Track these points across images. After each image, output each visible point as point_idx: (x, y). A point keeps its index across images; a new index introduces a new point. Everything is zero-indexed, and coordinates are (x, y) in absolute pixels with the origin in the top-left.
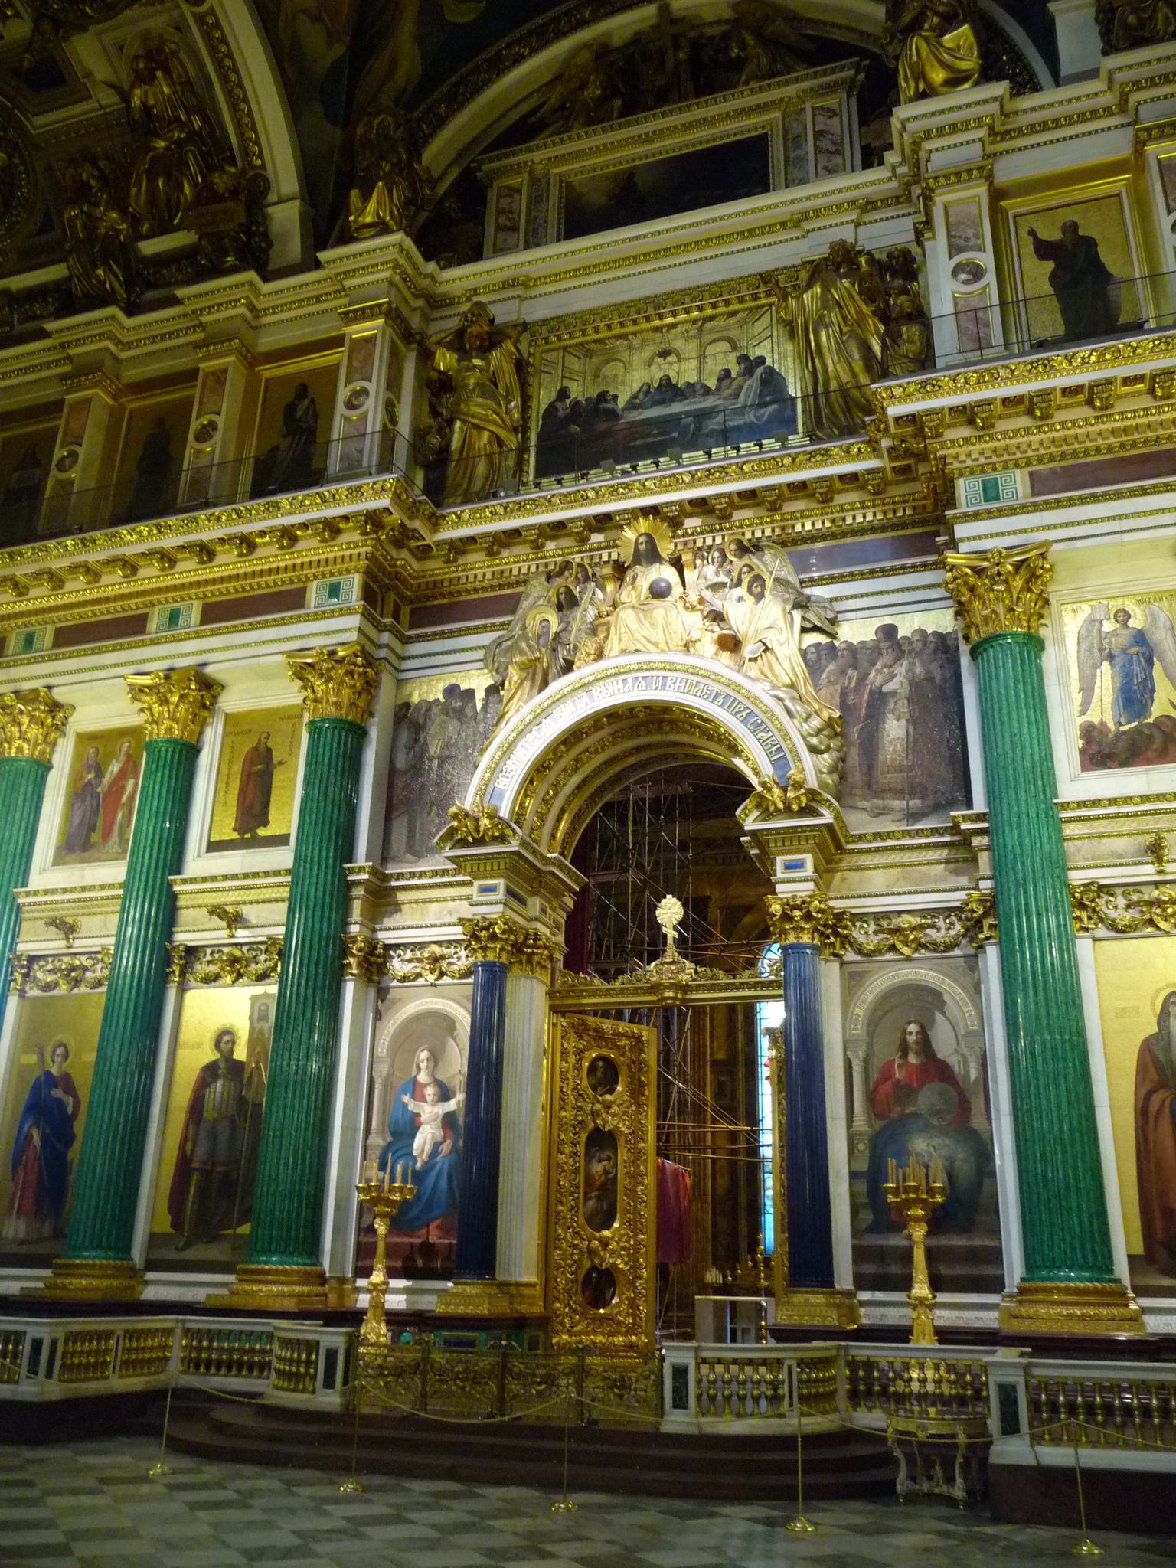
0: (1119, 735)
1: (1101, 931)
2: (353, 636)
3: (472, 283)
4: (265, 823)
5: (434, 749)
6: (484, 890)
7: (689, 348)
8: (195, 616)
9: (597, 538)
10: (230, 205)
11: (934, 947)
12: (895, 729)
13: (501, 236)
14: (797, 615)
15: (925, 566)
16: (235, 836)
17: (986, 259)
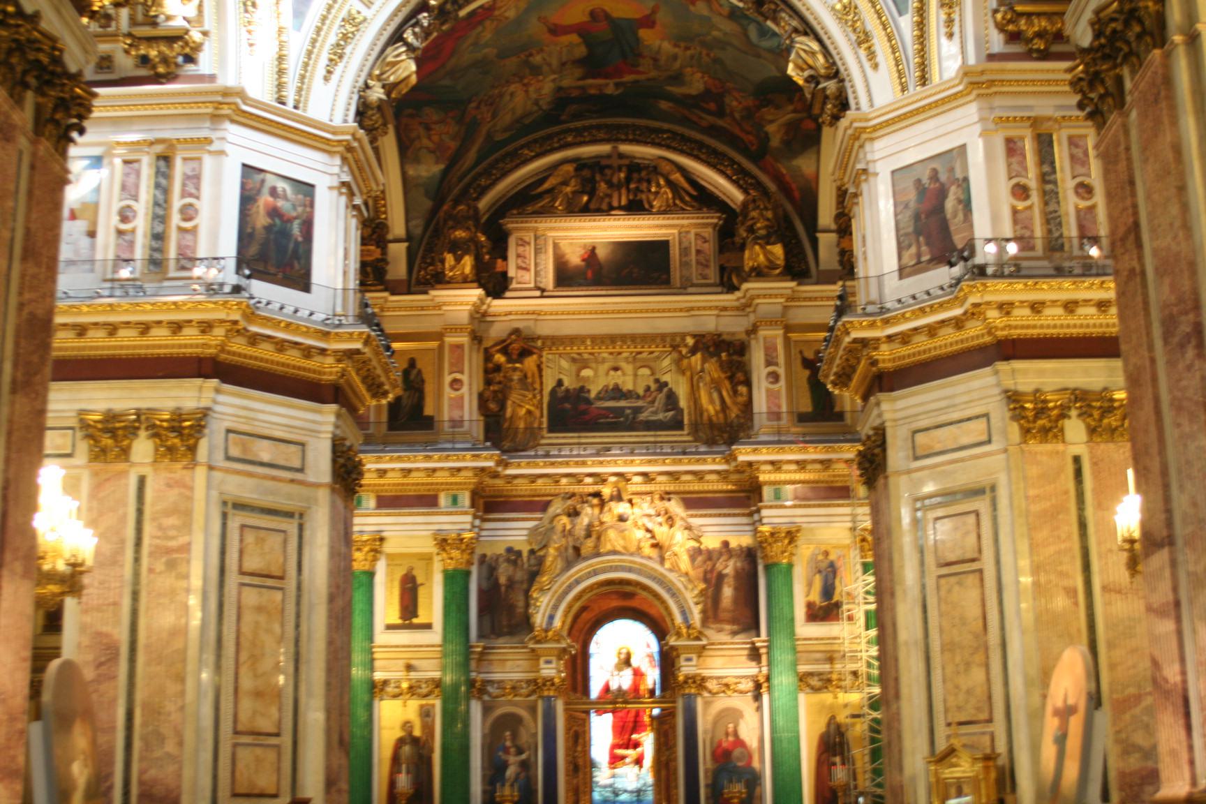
0: (821, 608)
1: (808, 690)
2: (468, 526)
3: (509, 309)
4: (416, 616)
5: (503, 580)
6: (548, 662)
7: (628, 368)
8: (372, 503)
9: (589, 480)
10: (372, 248)
11: (741, 692)
12: (728, 592)
13: (521, 273)
14: (686, 532)
15: (743, 515)
16: (399, 622)
17: (781, 371)
